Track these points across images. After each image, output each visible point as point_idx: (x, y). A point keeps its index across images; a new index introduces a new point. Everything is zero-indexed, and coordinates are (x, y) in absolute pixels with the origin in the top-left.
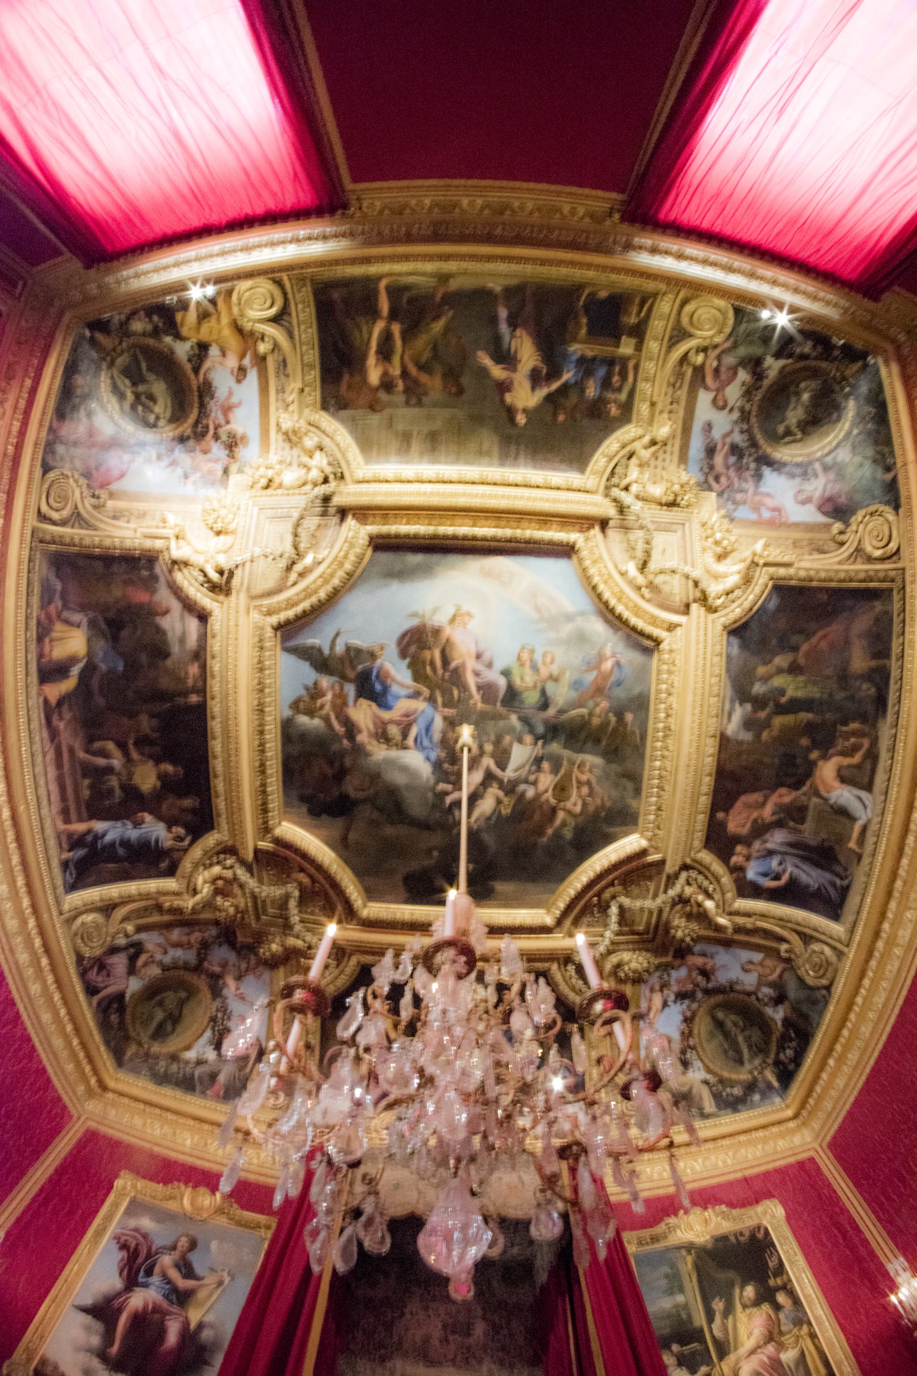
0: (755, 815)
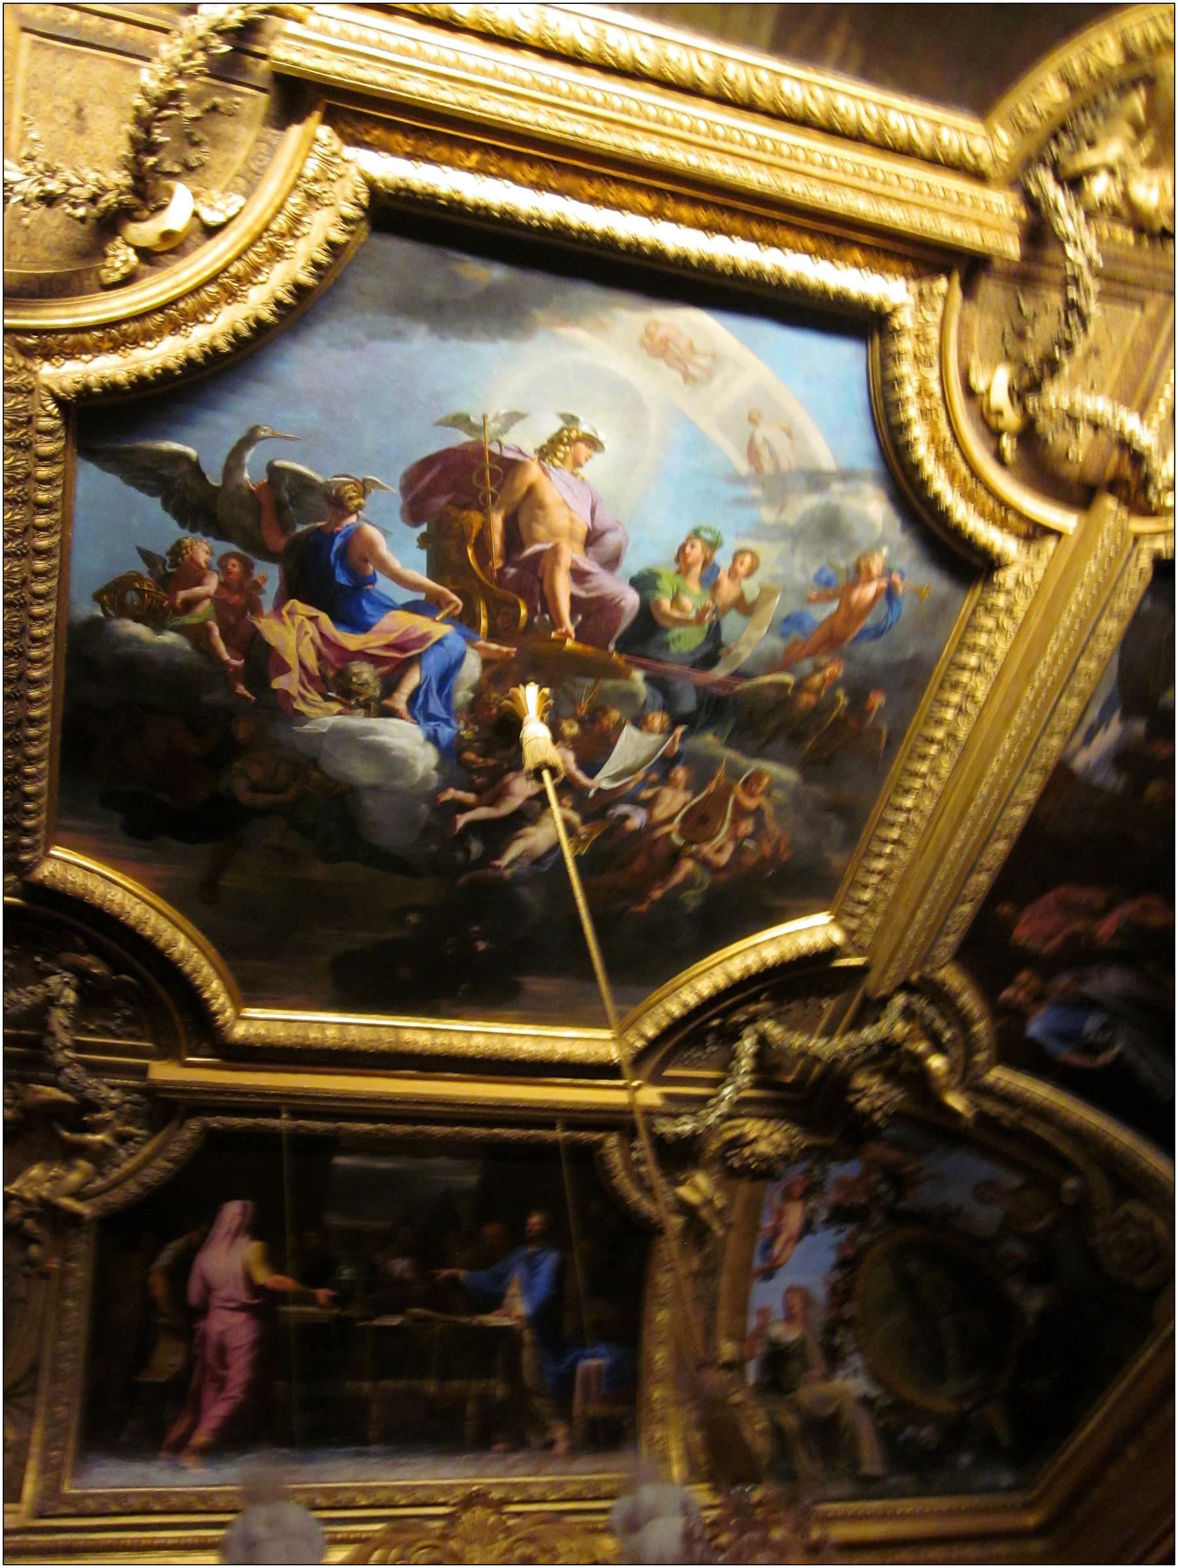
0: (1078, 926)
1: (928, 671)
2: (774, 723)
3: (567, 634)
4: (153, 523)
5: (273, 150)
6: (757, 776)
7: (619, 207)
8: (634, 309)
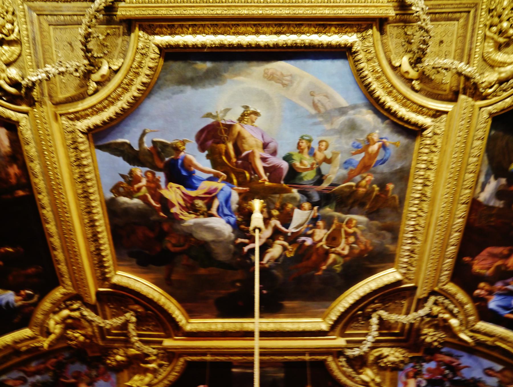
0: (499, 263)
1: (408, 172)
2: (351, 201)
3: (265, 180)
4: (123, 166)
5: (128, 43)
6: (350, 221)
7: (243, 34)
8: (258, 66)
